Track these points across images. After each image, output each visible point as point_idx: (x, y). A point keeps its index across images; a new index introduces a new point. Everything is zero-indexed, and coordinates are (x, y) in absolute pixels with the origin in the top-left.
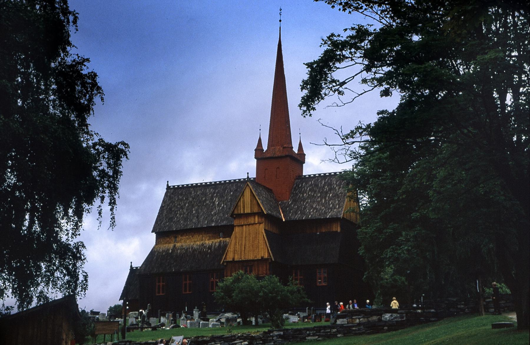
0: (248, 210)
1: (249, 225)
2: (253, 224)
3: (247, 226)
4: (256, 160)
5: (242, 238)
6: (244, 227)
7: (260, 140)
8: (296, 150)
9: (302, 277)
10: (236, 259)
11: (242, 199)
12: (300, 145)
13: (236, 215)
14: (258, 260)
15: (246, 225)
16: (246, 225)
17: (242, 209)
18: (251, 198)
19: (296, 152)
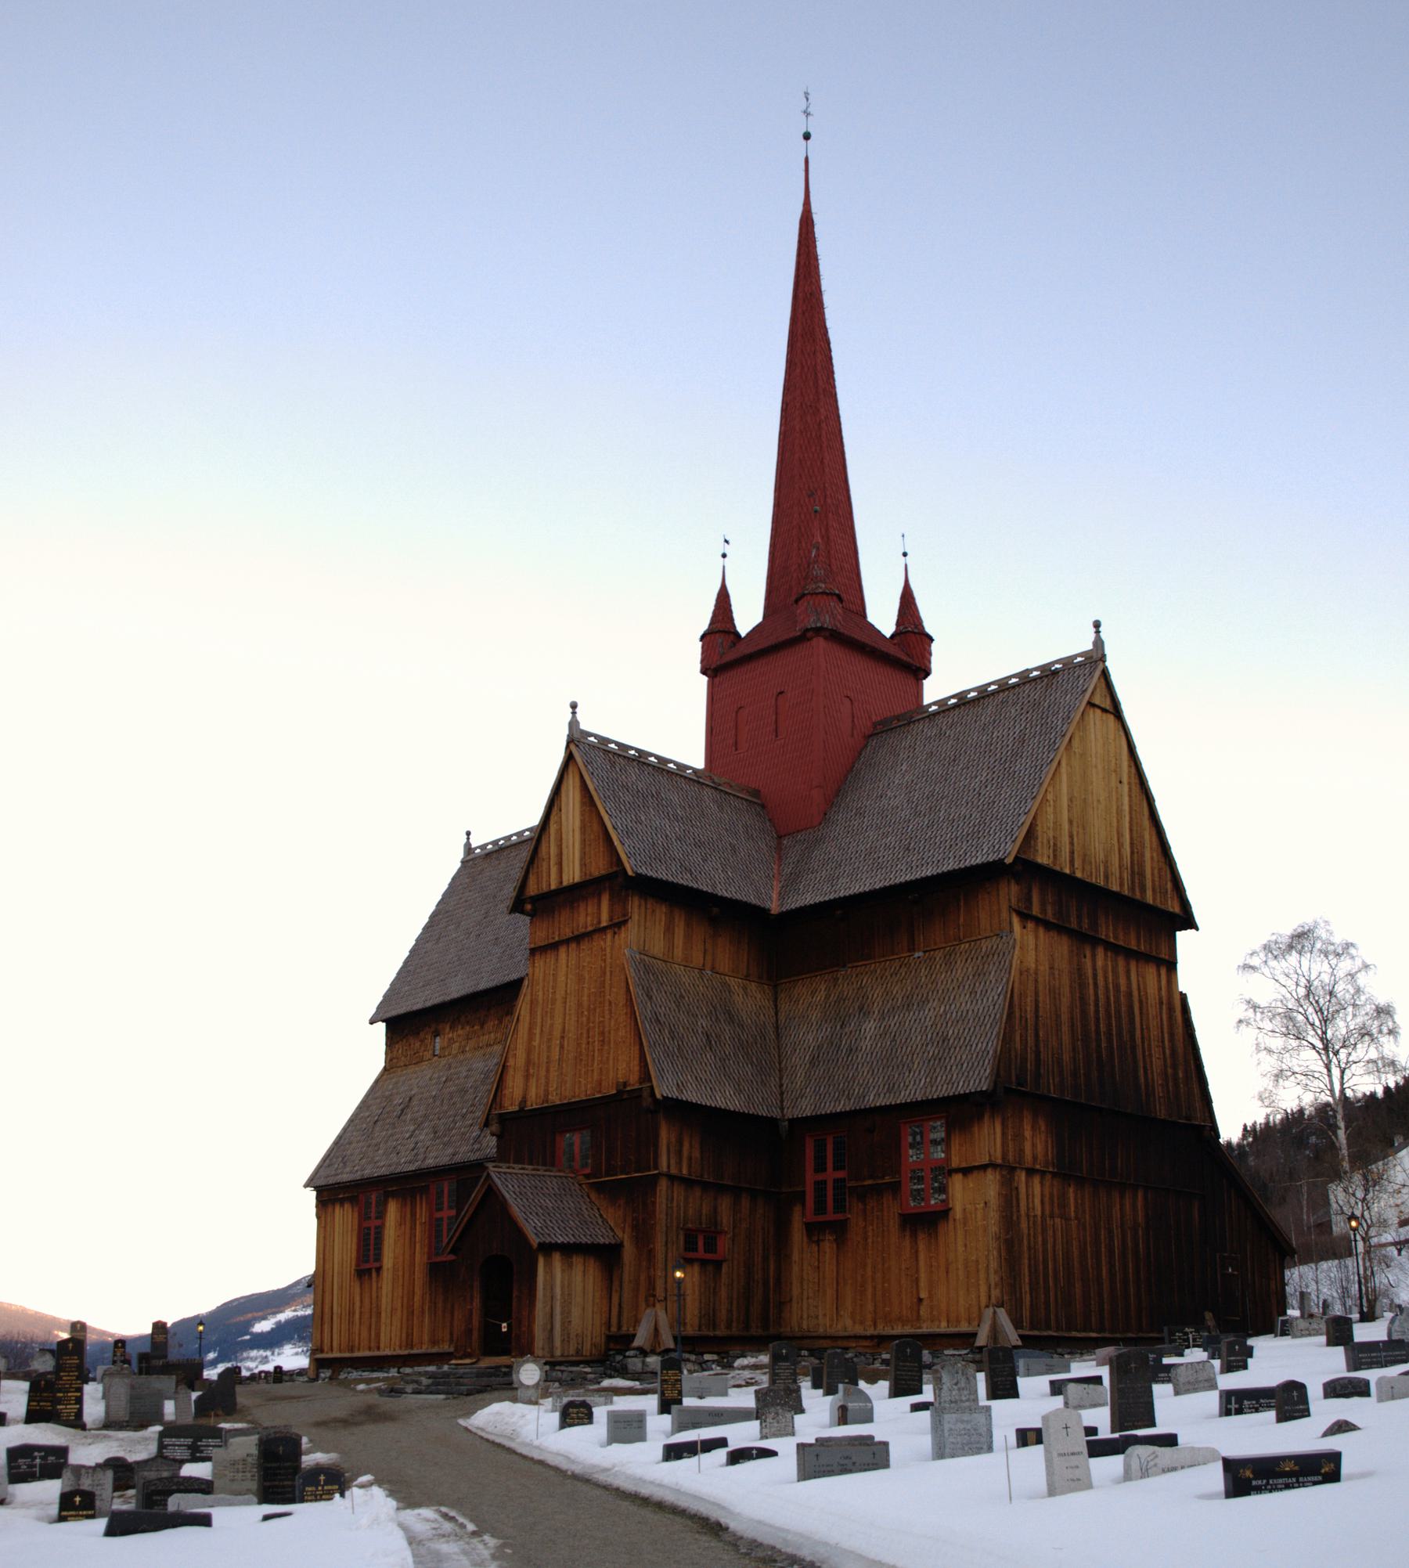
0: (573, 874)
1: (578, 939)
3: (573, 945)
4: (705, 679)
5: (554, 1001)
6: (563, 950)
8: (883, 617)
9: (841, 1174)
10: (533, 1103)
11: (553, 827)
13: (535, 899)
14: (606, 1100)
15: (567, 942)
16: (567, 942)
17: (554, 870)
18: (582, 814)
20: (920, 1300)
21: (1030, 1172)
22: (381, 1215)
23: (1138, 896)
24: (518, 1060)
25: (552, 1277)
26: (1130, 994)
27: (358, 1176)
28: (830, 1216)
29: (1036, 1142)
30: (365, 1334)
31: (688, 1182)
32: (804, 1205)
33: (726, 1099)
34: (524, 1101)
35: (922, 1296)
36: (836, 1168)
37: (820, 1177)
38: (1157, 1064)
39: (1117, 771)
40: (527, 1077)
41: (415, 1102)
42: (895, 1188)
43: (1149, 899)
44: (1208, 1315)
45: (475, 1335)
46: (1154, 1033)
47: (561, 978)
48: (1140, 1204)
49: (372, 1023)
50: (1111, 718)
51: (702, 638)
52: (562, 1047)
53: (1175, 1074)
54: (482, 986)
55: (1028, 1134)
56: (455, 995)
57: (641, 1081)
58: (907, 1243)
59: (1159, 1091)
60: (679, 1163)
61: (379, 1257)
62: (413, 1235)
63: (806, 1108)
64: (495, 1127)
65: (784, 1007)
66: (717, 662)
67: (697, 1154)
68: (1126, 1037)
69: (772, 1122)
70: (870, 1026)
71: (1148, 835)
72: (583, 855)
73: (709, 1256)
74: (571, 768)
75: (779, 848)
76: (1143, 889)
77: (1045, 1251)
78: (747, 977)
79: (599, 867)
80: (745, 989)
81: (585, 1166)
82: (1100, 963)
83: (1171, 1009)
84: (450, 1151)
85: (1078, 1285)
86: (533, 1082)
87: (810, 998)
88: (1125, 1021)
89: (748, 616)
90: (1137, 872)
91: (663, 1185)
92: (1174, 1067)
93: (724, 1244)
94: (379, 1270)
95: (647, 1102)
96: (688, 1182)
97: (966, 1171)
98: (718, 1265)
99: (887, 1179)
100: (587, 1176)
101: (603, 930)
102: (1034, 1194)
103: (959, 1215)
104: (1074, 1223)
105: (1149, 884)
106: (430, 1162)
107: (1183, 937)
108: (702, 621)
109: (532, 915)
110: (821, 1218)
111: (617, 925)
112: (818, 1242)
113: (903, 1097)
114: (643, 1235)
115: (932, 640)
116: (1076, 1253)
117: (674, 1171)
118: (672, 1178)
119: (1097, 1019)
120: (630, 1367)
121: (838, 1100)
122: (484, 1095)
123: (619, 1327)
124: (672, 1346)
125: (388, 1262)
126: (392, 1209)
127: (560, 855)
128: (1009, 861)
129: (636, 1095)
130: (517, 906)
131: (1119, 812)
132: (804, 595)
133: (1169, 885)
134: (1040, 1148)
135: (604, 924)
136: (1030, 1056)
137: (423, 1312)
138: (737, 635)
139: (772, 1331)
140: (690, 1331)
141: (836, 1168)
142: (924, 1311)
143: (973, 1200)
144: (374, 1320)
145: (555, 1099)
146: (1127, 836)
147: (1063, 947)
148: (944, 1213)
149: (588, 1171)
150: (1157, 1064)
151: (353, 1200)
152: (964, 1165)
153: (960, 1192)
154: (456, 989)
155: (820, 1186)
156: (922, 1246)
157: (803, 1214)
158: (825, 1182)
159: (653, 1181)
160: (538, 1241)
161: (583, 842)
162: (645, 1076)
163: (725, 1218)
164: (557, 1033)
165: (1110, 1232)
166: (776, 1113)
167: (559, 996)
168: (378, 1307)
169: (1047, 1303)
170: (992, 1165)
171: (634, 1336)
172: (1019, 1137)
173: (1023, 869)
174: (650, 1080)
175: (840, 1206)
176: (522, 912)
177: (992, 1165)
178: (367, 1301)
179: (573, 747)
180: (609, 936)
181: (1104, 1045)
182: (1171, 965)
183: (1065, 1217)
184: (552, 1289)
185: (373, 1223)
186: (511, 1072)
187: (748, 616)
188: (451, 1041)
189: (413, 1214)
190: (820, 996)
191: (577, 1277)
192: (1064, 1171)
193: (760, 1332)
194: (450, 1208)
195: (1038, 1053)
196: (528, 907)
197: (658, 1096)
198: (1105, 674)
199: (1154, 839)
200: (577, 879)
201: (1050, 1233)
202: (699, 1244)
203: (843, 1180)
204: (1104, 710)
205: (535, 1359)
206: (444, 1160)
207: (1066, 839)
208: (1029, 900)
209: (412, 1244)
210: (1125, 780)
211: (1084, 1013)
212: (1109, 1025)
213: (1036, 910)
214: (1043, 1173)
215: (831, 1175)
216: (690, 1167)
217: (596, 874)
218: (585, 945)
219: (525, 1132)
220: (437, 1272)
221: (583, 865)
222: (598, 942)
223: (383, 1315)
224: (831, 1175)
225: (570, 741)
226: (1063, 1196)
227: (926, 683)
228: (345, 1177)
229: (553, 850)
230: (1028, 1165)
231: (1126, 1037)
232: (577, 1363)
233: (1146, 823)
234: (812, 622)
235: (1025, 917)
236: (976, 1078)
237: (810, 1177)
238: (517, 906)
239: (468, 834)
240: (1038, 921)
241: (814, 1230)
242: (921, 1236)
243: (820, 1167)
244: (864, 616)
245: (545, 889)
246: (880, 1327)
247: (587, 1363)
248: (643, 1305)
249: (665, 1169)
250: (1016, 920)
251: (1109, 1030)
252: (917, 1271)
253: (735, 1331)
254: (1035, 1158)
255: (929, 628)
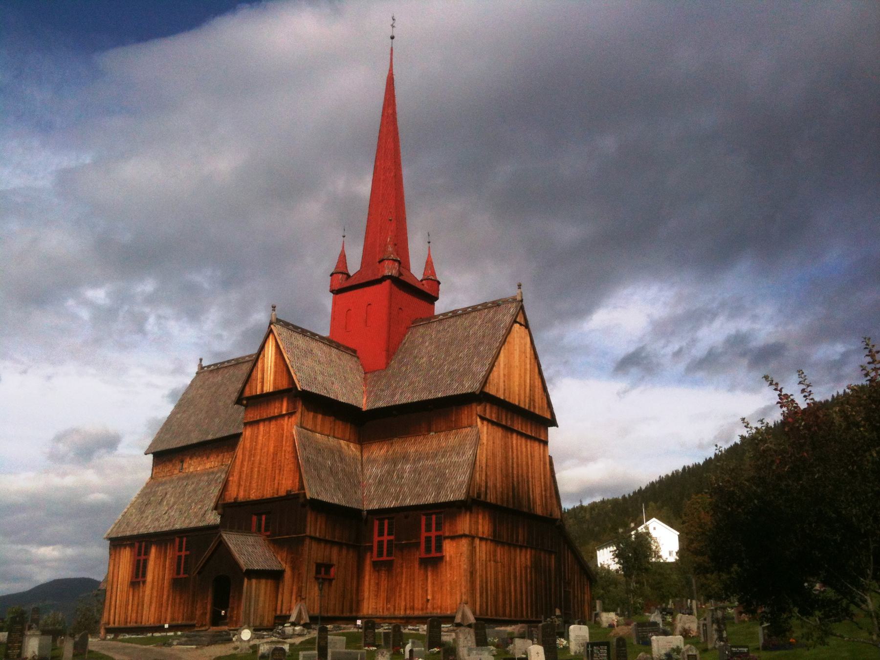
0: (269, 387)
2: (275, 418)
3: (267, 423)
5: (255, 449)
7: (343, 258)
8: (417, 270)
9: (392, 538)
11: (259, 365)
12: (429, 264)
14: (281, 499)
16: (264, 420)
18: (276, 359)
19: (419, 277)
20: (428, 600)
21: (481, 539)
22: (147, 553)
23: (532, 410)
24: (234, 479)
25: (251, 585)
26: (527, 456)
27: (135, 533)
28: (385, 558)
29: (483, 526)
30: (134, 615)
31: (319, 540)
32: (372, 552)
33: (337, 499)
34: (236, 499)
35: (429, 597)
36: (389, 535)
37: (381, 538)
38: (538, 491)
39: (525, 353)
40: (239, 485)
41: (168, 496)
42: (417, 545)
43: (537, 411)
44: (558, 612)
45: (208, 616)
46: (537, 475)
47: (260, 438)
48: (528, 557)
49: (146, 454)
50: (523, 328)
51: (332, 275)
52: (259, 471)
53: (546, 497)
54: (210, 437)
55: (480, 521)
56: (195, 441)
57: (299, 490)
58: (422, 572)
59: (538, 502)
60: (315, 530)
61: (144, 575)
62: (164, 566)
63: (375, 505)
64: (220, 510)
65: (365, 457)
66: (337, 287)
67: (323, 526)
68: (525, 477)
69: (358, 512)
70: (408, 467)
71: (538, 382)
72: (275, 379)
73: (326, 577)
74: (271, 337)
75: (365, 379)
76: (534, 407)
77: (487, 578)
78: (348, 440)
79: (284, 385)
80: (348, 446)
81: (266, 530)
82: (514, 442)
83: (545, 464)
84: (187, 521)
85: (501, 595)
86: (242, 488)
87: (378, 451)
88: (525, 468)
89: (354, 266)
90: (532, 400)
91: (307, 541)
92: (545, 490)
93: (333, 571)
94: (144, 582)
95: (302, 500)
96: (319, 540)
97: (453, 538)
98: (330, 581)
99: (414, 541)
100: (268, 536)
101: (282, 416)
102: (482, 549)
103: (448, 559)
104: (499, 564)
105: (537, 405)
106: (178, 526)
107: (551, 430)
108: (330, 265)
109: (246, 406)
110: (381, 559)
111: (290, 414)
112: (378, 571)
113: (423, 501)
114: (295, 566)
115: (439, 283)
116: (500, 577)
117: (313, 534)
118: (311, 538)
119: (513, 468)
120: (287, 632)
121: (391, 502)
122: (215, 491)
123: (281, 611)
124: (308, 621)
125: (149, 578)
126: (153, 550)
127: (263, 378)
128: (478, 393)
129: (296, 496)
130: (239, 401)
131: (525, 369)
132: (383, 260)
133: (546, 406)
134: (486, 527)
135: (284, 412)
136: (483, 484)
137: (168, 604)
138: (348, 276)
139: (354, 614)
140: (316, 612)
141: (389, 535)
142: (429, 606)
143: (454, 552)
144: (140, 608)
145: (253, 497)
146: (528, 381)
147: (499, 433)
148: (441, 558)
149: (268, 533)
150: (538, 491)
151: (131, 546)
152: (451, 535)
153: (449, 548)
154: (195, 438)
155: (380, 543)
156: (429, 574)
157: (371, 557)
158: (382, 541)
159: (303, 539)
160: (245, 569)
161: (275, 372)
162: (302, 487)
163: (335, 557)
164: (256, 465)
165: (515, 568)
166: (361, 508)
167: (259, 447)
168: (143, 601)
169: (487, 603)
170: (465, 536)
171: (289, 616)
172: (477, 523)
173: (482, 397)
174: (304, 489)
175: (390, 553)
176: (242, 404)
177: (465, 536)
178: (136, 598)
179: (272, 326)
180: (286, 419)
181: (515, 479)
182: (546, 443)
183: (496, 561)
184: (251, 593)
185: (142, 557)
186: (230, 483)
187: (354, 266)
188: (190, 465)
189: (165, 553)
190: (382, 452)
191: (263, 586)
192: (496, 539)
193: (348, 614)
194: (186, 550)
195: (486, 483)
196: (245, 402)
197: (308, 498)
198: (522, 308)
199: (540, 386)
200: (271, 390)
201: (489, 569)
202: (323, 571)
203: (392, 540)
204: (521, 325)
205: (249, 627)
206: (184, 526)
207: (502, 384)
208: (485, 411)
209: (164, 566)
210: (528, 355)
211: (507, 464)
212: (518, 470)
213: (488, 416)
214: (486, 540)
215: (386, 538)
216: (320, 532)
217: (281, 388)
218: (273, 424)
219: (236, 513)
220: (178, 584)
221: (275, 383)
222: (280, 421)
223: (145, 606)
224: (386, 538)
225: (271, 323)
226: (495, 551)
227: (436, 303)
228: (128, 534)
229: (259, 376)
230: (480, 535)
231: (525, 477)
232: (259, 630)
233: (537, 376)
234: (387, 273)
235: (483, 419)
236: (459, 495)
237: (376, 539)
238: (239, 401)
239: (201, 360)
240: (489, 421)
241: (376, 566)
242: (430, 569)
243: (381, 534)
244: (409, 270)
245: (254, 394)
246: (408, 612)
247: (265, 630)
248: (294, 601)
249: (308, 533)
250: (478, 420)
251: (518, 472)
252: (427, 586)
253: (337, 614)
254: (483, 533)
255: (439, 278)
